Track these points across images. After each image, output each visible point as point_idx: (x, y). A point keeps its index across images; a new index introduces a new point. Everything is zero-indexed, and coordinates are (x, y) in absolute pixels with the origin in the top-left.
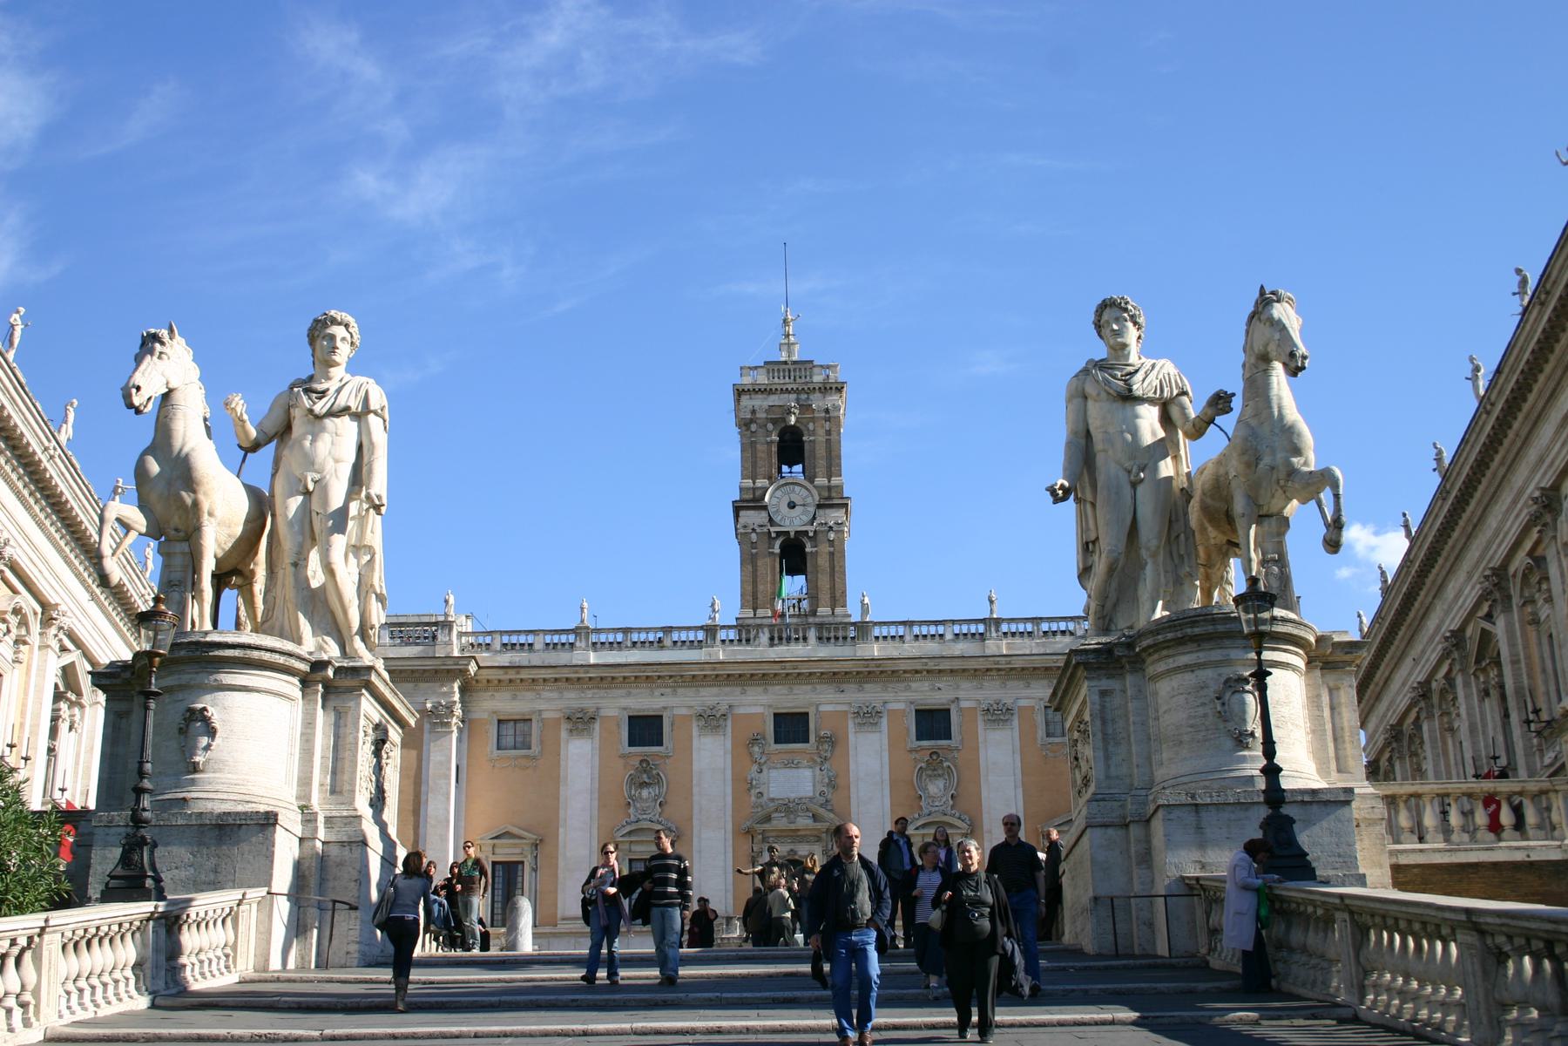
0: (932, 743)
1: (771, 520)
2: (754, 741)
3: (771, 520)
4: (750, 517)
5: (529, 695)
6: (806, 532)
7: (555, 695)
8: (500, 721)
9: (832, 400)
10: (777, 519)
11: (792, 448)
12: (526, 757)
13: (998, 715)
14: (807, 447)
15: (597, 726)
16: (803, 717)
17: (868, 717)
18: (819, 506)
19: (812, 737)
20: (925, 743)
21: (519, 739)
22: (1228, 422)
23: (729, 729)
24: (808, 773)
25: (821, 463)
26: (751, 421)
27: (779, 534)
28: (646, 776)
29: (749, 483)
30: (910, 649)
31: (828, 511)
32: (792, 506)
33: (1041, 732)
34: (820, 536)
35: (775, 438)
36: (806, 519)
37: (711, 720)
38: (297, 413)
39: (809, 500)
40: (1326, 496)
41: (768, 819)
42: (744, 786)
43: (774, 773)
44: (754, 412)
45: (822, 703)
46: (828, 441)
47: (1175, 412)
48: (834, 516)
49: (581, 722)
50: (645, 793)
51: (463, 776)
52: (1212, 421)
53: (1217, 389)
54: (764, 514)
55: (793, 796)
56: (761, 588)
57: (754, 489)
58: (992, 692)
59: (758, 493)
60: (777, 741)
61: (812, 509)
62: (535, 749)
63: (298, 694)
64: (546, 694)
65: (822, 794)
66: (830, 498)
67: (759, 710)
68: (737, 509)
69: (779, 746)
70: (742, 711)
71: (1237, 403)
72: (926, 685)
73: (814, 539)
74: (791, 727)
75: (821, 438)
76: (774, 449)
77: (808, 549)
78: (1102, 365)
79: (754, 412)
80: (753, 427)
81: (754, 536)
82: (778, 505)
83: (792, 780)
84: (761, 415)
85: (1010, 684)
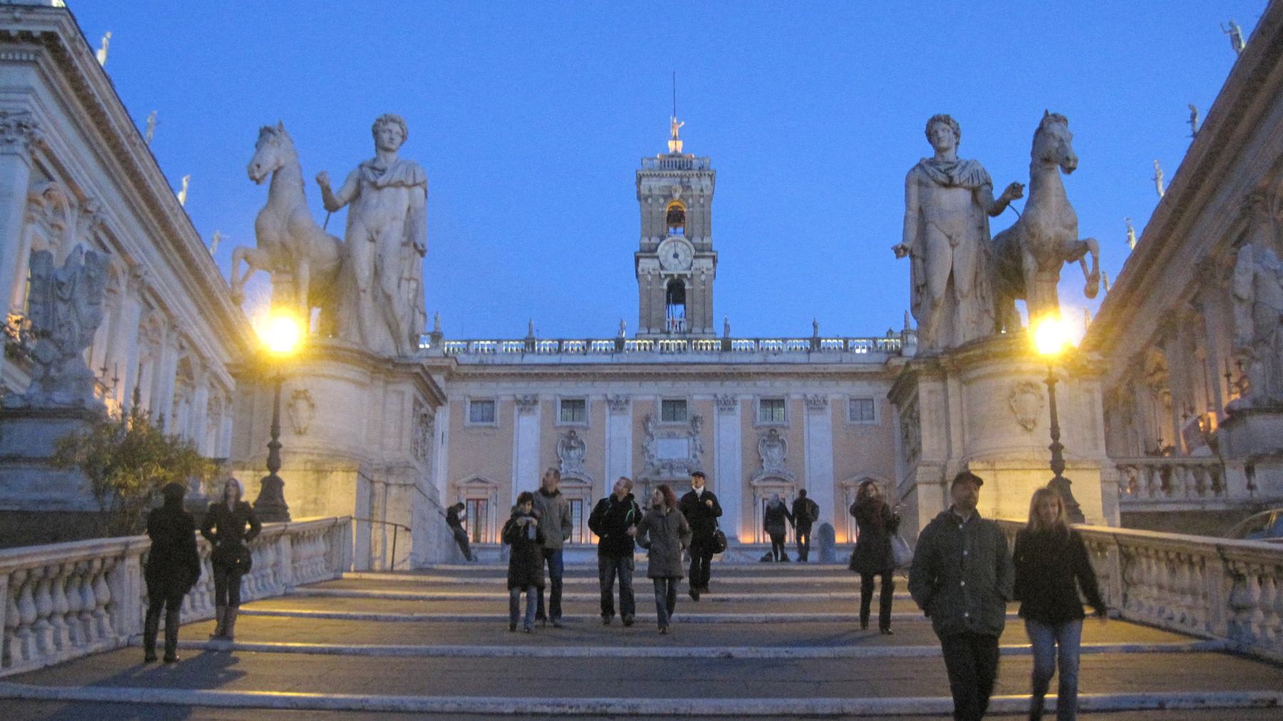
2: (647, 419)
3: (662, 267)
4: (647, 264)
5: (493, 385)
7: (510, 385)
9: (706, 182)
10: (666, 265)
12: (491, 427)
13: (816, 405)
15: (539, 406)
16: (682, 403)
17: (726, 404)
18: (695, 257)
21: (486, 414)
22: (1019, 205)
24: (685, 442)
27: (666, 276)
28: (571, 440)
29: (646, 241)
30: (757, 358)
34: (696, 279)
36: (685, 265)
37: (617, 404)
38: (365, 183)
40: (1088, 257)
41: (658, 473)
42: (642, 450)
43: (660, 442)
47: (981, 196)
48: (707, 263)
49: (526, 404)
50: (572, 453)
51: (446, 439)
52: (1008, 203)
53: (1009, 183)
54: (656, 262)
55: (674, 458)
58: (814, 389)
61: (689, 259)
62: (498, 420)
63: (368, 381)
64: (504, 384)
65: (695, 456)
67: (652, 398)
70: (640, 398)
71: (1026, 192)
72: (768, 384)
73: (691, 279)
74: (674, 407)
75: (697, 209)
77: (687, 287)
78: (932, 162)
80: (650, 201)
81: (649, 278)
84: (656, 192)
85: (826, 383)
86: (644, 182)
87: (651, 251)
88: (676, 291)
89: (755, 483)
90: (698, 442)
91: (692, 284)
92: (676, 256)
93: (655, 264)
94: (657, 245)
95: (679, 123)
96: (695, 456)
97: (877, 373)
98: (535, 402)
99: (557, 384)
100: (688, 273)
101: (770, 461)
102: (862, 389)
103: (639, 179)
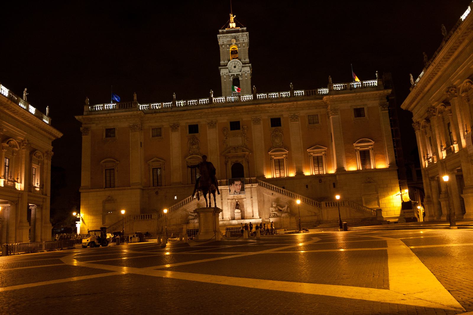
1: (230, 72)
3: (230, 72)
8: (152, 129)
10: (231, 71)
15: (179, 128)
16: (238, 123)
18: (243, 67)
19: (241, 128)
20: (274, 128)
23: (217, 127)
24: (240, 138)
26: (223, 45)
27: (232, 75)
32: (235, 67)
34: (243, 75)
36: (239, 70)
39: (240, 65)
44: (223, 42)
49: (175, 127)
50: (194, 147)
54: (227, 70)
59: (226, 64)
60: (231, 129)
67: (226, 121)
69: (233, 131)
74: (235, 126)
77: (240, 79)
79: (223, 42)
80: (223, 46)
81: (225, 77)
82: (231, 67)
83: (236, 140)
92: (235, 67)
93: (227, 71)
95: (233, 16)
100: (240, 73)
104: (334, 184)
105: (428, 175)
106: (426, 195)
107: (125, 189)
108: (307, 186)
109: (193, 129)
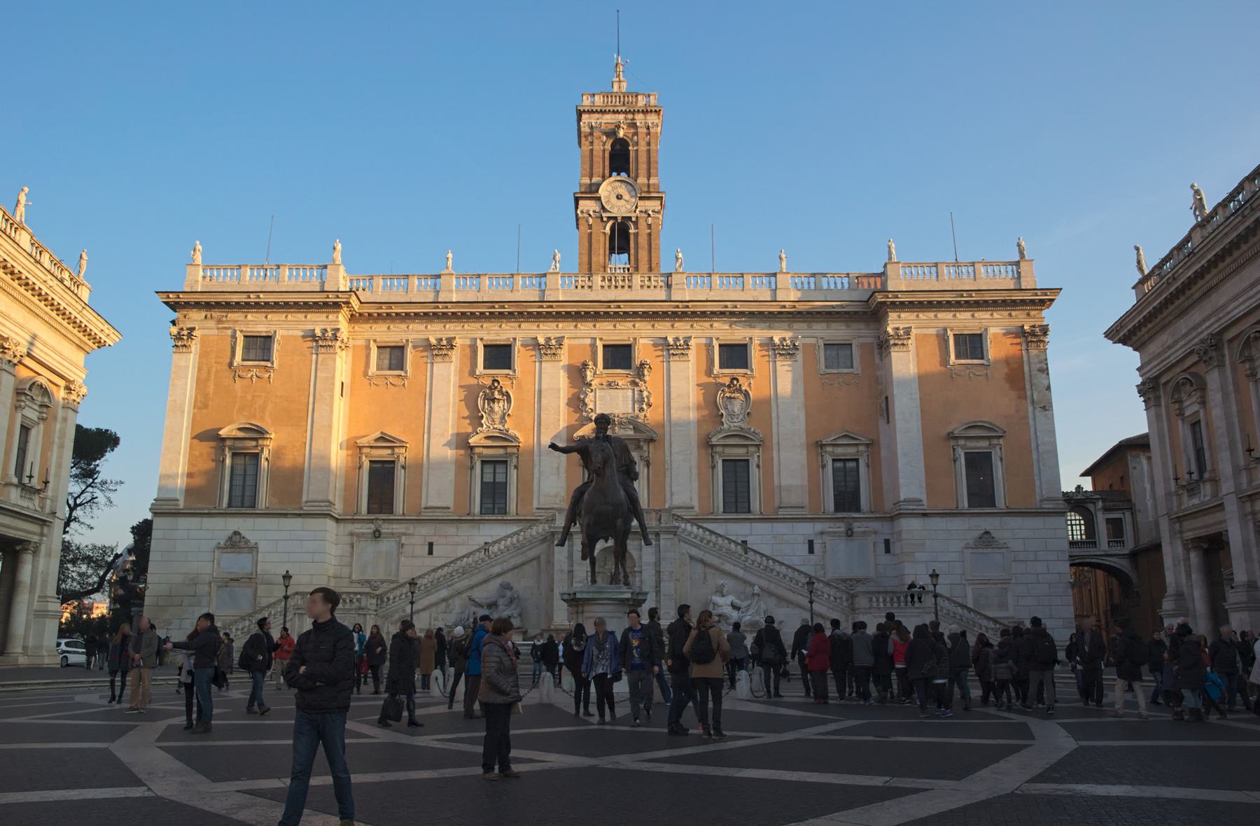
0: (732, 371)
3: (603, 208)
4: (588, 206)
6: (630, 218)
11: (620, 159)
14: (632, 154)
18: (641, 198)
25: (643, 167)
27: (609, 218)
29: (586, 181)
31: (648, 203)
32: (619, 197)
33: (823, 366)
34: (642, 223)
35: (608, 147)
42: (577, 403)
45: (642, 337)
46: (649, 151)
50: (496, 407)
56: (594, 259)
57: (591, 185)
59: (594, 188)
65: (641, 410)
66: (649, 192)
68: (577, 200)
73: (636, 223)
76: (607, 155)
77: (632, 231)
86: (584, 116)
87: (591, 191)
88: (621, 237)
89: (714, 441)
90: (645, 394)
91: (636, 228)
94: (599, 185)
96: (641, 410)
97: (856, 313)
98: (452, 347)
99: (478, 325)
100: (632, 215)
101: (732, 415)
102: (838, 332)
103: (580, 114)
104: (887, 542)
105: (1181, 532)
106: (1171, 590)
107: (285, 515)
108: (811, 543)
109: (499, 356)
